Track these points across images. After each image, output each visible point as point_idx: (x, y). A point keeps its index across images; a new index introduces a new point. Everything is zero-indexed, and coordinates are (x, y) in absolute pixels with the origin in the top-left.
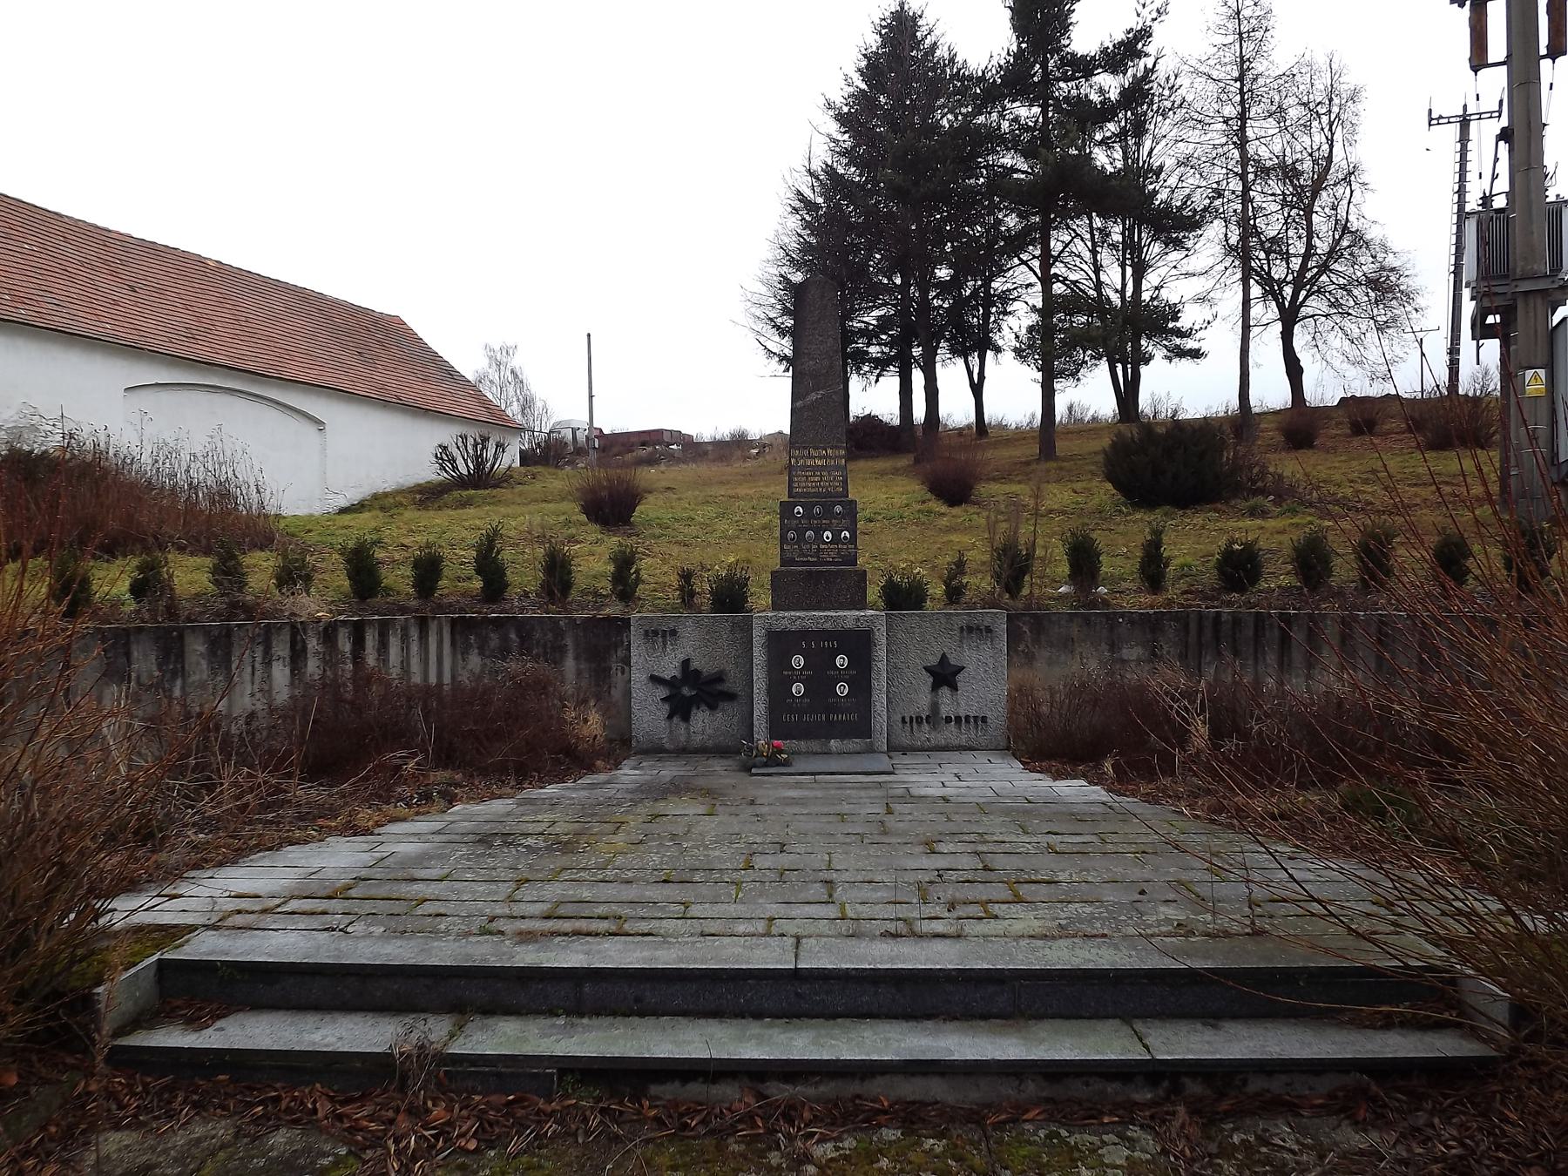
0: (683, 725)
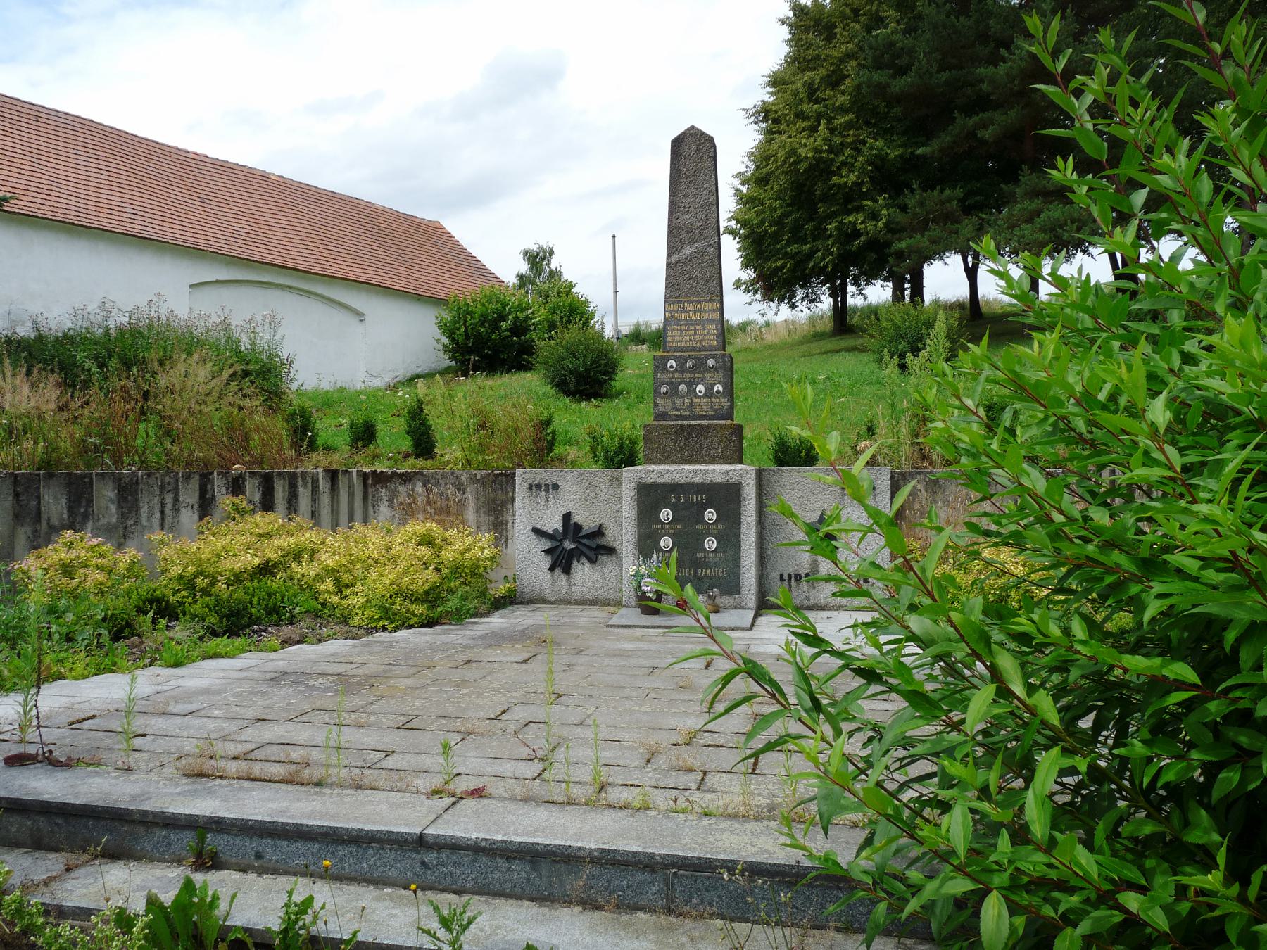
0: (563, 577)
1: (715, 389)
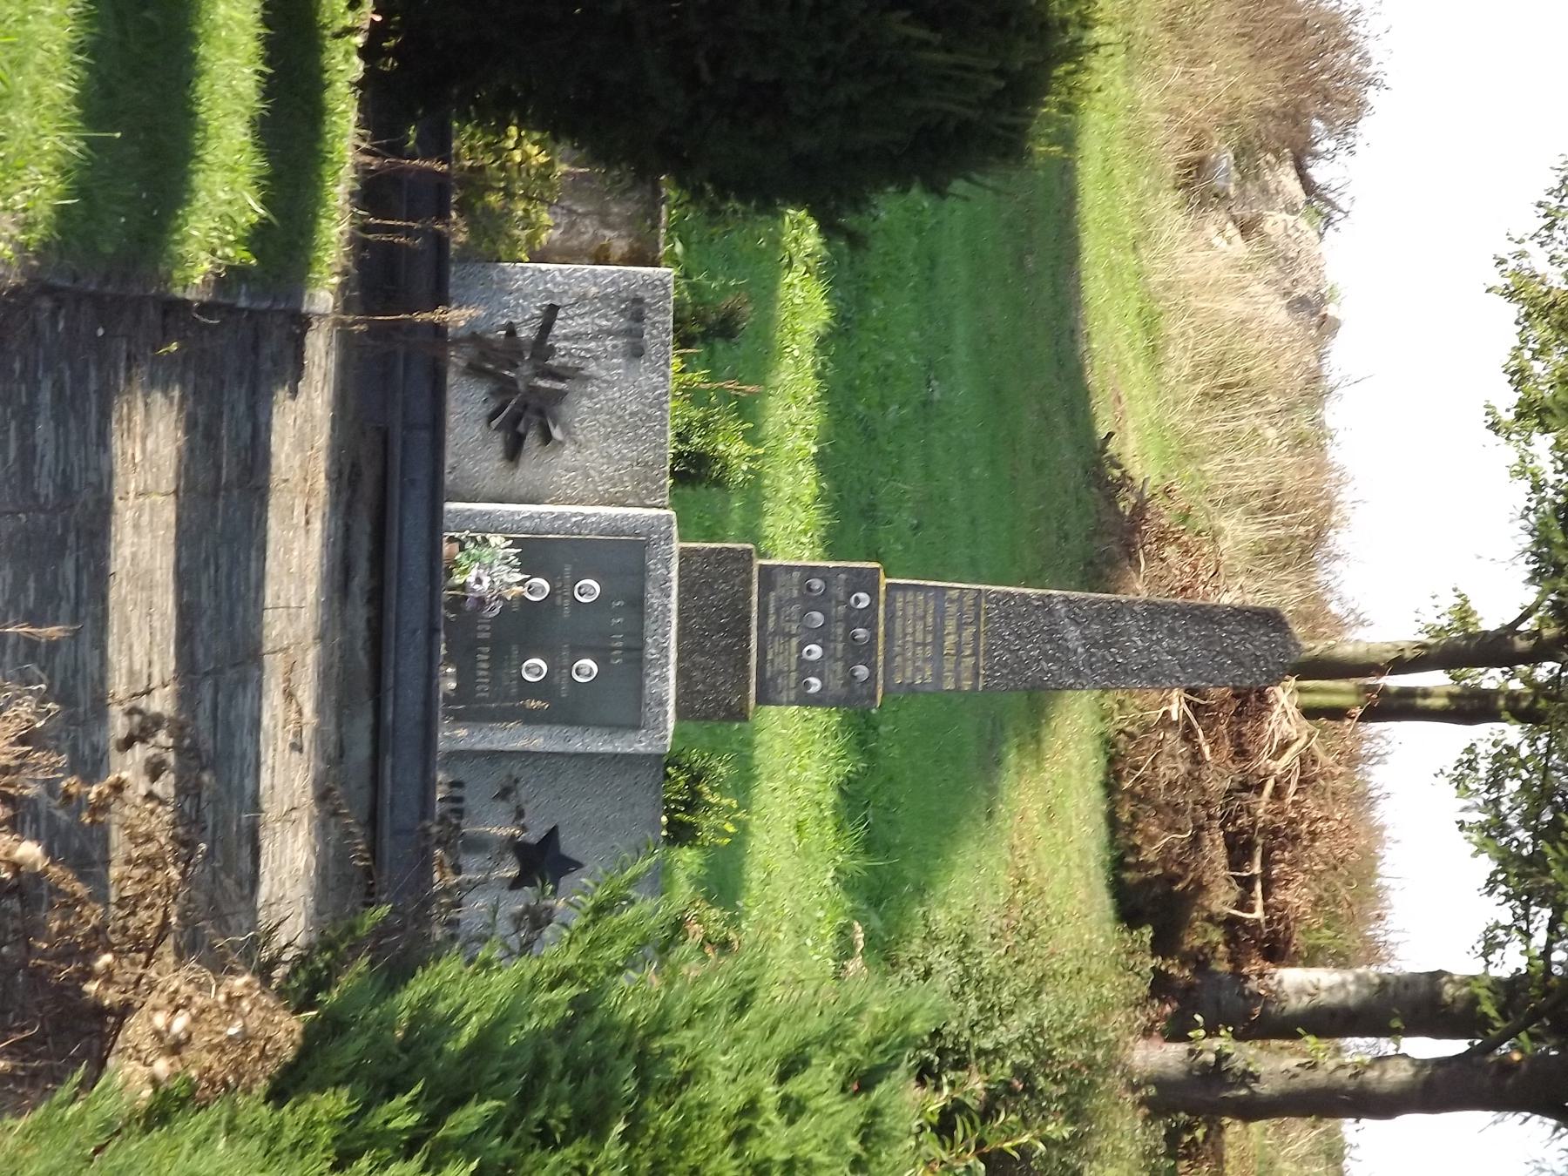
1: (813, 680)
